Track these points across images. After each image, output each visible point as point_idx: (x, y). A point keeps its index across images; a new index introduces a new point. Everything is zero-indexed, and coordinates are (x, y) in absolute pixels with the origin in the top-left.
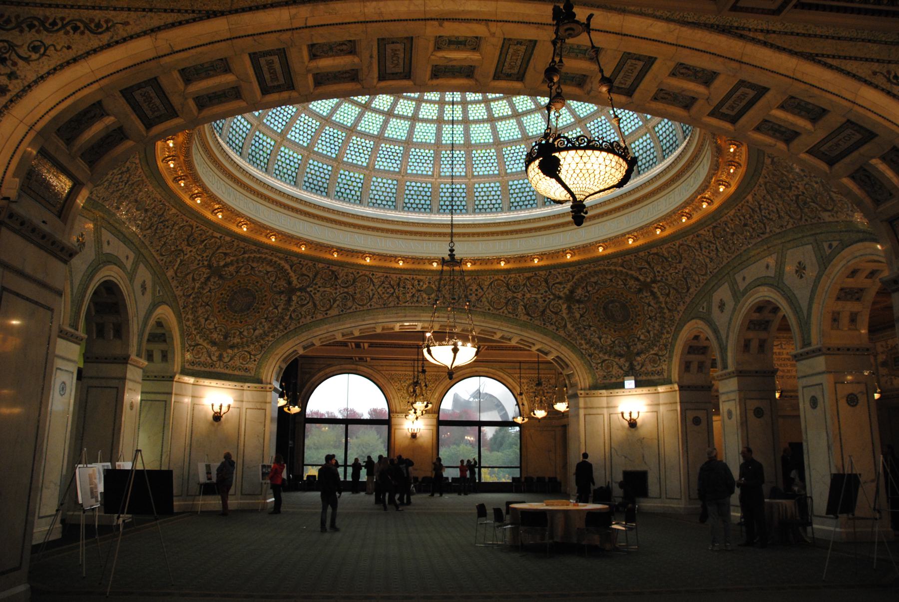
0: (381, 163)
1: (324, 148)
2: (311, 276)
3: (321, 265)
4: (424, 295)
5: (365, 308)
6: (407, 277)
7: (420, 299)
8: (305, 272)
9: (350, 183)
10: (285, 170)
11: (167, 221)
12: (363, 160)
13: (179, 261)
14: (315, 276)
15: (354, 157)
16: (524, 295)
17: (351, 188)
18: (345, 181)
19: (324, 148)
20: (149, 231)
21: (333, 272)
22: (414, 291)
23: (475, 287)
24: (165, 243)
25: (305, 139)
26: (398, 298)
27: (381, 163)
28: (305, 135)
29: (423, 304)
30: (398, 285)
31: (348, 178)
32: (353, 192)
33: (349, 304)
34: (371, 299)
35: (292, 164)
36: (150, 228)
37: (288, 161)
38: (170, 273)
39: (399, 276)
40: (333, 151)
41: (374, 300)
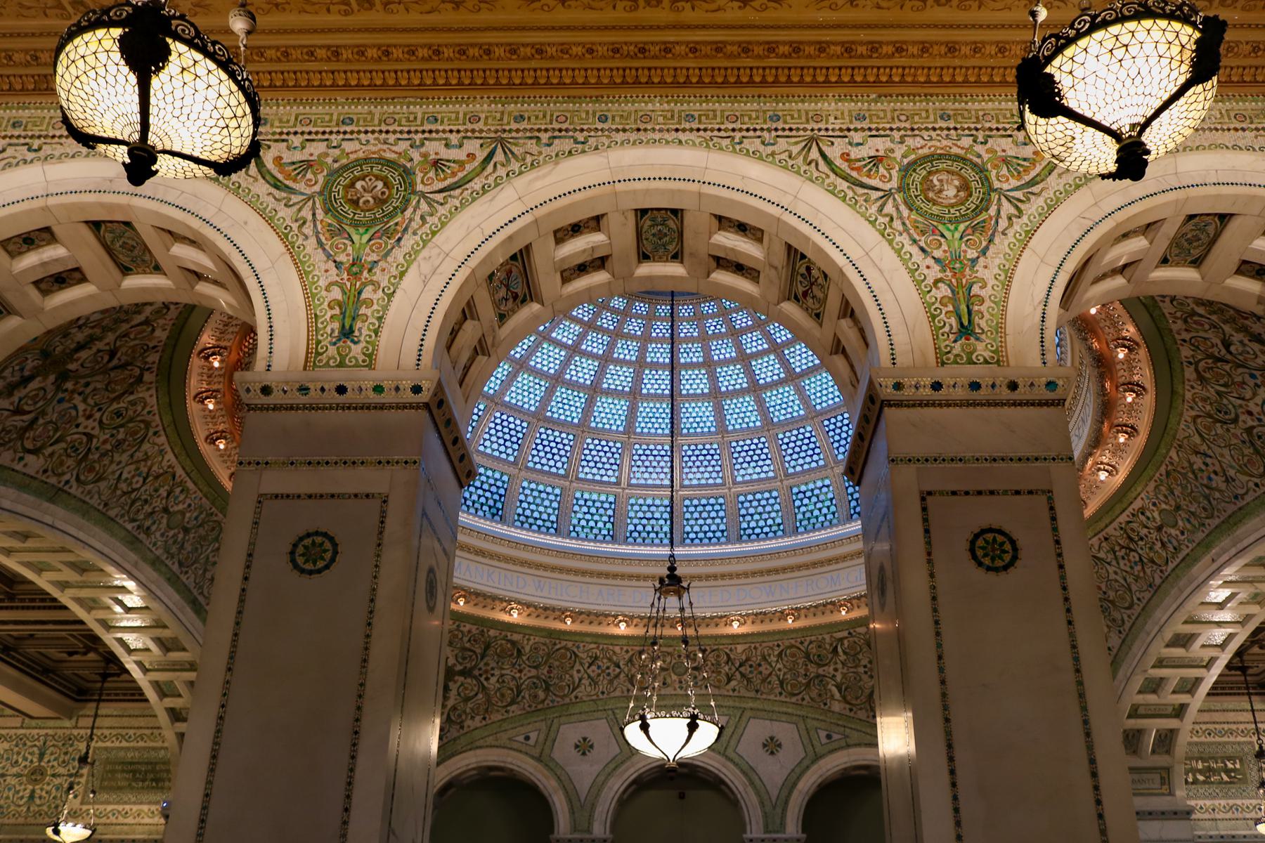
4: (1173, 532)
5: (1137, 609)
6: (1123, 518)
7: (1175, 543)
11: (747, 660)
13: (834, 690)
16: (1250, 413)
20: (733, 683)
22: (1154, 535)
23: (1198, 462)
24: (781, 683)
26: (1153, 562)
29: (1185, 551)
30: (1131, 539)
33: (1117, 615)
34: (1130, 590)
36: (729, 680)
38: (837, 707)
39: (1115, 524)
41: (1134, 588)
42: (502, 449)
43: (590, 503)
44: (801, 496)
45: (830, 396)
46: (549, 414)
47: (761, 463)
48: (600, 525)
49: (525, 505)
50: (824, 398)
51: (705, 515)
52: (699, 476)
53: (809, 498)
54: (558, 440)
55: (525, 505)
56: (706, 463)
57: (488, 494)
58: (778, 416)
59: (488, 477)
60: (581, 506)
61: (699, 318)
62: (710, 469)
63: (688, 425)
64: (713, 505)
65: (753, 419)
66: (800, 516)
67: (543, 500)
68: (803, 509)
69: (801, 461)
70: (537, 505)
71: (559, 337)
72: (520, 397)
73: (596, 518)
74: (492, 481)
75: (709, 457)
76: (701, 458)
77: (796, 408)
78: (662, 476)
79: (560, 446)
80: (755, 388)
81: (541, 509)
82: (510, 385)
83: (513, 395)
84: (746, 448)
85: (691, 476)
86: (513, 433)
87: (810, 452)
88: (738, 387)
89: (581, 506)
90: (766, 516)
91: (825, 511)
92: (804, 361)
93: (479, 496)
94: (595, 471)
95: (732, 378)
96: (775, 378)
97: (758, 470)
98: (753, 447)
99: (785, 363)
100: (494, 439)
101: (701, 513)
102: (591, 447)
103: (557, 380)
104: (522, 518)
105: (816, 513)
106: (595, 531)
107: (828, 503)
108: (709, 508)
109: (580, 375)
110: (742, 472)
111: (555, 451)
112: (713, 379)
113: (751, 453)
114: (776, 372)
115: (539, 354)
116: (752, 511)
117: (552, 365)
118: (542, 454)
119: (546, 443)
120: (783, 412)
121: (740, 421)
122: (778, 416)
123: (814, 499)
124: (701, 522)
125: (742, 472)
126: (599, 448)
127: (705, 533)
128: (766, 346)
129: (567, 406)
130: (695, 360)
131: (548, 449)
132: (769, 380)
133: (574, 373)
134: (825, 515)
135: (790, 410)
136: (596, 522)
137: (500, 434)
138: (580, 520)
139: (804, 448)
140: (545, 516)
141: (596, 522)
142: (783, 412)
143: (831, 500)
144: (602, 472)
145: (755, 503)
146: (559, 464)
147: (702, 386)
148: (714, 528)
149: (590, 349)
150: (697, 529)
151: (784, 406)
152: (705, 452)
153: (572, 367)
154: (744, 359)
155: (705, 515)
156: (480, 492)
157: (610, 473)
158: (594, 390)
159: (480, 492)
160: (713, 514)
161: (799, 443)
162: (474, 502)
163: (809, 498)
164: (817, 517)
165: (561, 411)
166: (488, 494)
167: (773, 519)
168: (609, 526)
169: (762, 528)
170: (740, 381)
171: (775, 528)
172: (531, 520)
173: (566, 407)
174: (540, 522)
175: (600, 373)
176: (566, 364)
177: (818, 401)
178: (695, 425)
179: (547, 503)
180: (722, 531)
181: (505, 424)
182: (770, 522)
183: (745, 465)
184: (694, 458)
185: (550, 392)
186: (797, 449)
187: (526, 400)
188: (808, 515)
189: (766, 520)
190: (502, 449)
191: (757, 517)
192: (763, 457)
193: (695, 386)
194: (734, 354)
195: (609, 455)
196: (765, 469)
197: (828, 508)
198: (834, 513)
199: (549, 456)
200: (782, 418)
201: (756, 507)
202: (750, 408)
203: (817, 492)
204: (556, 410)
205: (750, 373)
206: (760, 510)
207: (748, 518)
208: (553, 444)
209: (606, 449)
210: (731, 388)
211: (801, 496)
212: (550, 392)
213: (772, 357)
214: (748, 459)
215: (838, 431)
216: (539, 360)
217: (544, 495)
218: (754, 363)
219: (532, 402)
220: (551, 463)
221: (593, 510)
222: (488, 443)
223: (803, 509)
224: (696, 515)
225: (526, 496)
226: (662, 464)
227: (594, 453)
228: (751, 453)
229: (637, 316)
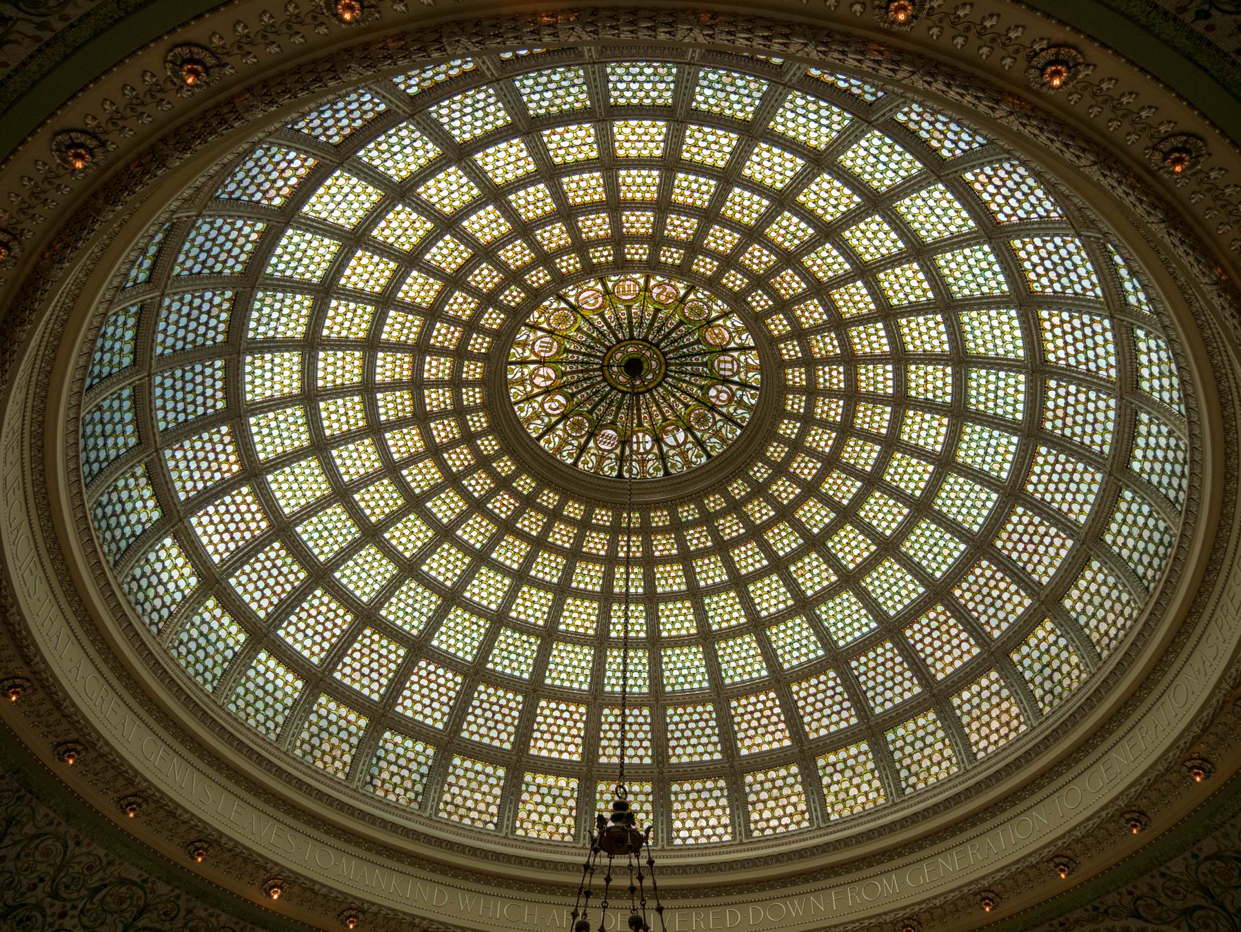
0: (1041, 569)
1: (948, 659)
2: (1203, 902)
3: (1176, 867)
8: (1179, 905)
9: (1046, 659)
10: (926, 763)
12: (1016, 599)
14: (1206, 891)
15: (1001, 615)
17: (1056, 664)
18: (1037, 666)
19: (948, 659)
21: (1216, 856)
25: (907, 684)
27: (1041, 569)
28: (899, 679)
31: (1035, 654)
32: (1065, 668)
35: (929, 739)
37: (919, 745)
40: (965, 646)
42: (428, 711)
43: (544, 790)
44: (830, 770)
45: (856, 625)
46: (490, 666)
47: (771, 728)
48: (558, 820)
49: (455, 790)
50: (848, 629)
51: (700, 804)
52: (690, 750)
53: (842, 772)
54: (503, 702)
55: (455, 790)
56: (698, 732)
57: (405, 773)
58: (790, 661)
59: (406, 749)
60: (532, 794)
61: (677, 528)
62: (704, 740)
63: (672, 680)
64: (710, 790)
65: (757, 667)
66: (830, 799)
67: (480, 784)
68: (834, 788)
69: (825, 722)
70: (473, 791)
71: (501, 559)
72: (452, 641)
73: (552, 810)
74: (411, 755)
75: (702, 724)
76: (692, 725)
77: (812, 647)
78: (641, 752)
79: (506, 711)
80: (757, 625)
81: (478, 796)
82: (440, 624)
83: (444, 638)
84: (750, 708)
85: (679, 751)
86: (442, 690)
87: (836, 708)
88: (733, 623)
89: (532, 794)
90: (783, 801)
91: (865, 787)
92: (817, 580)
93: (393, 774)
94: (551, 745)
95: (725, 611)
96: (781, 606)
97: (769, 738)
98: (760, 706)
99: (792, 585)
100: (417, 697)
101: (694, 801)
102: (547, 712)
103: (499, 619)
104: (449, 808)
105: (853, 791)
106: (549, 828)
107: (868, 777)
108: (705, 795)
109: (530, 612)
110: (747, 742)
111: (498, 717)
112: (701, 615)
113: (757, 715)
114: (782, 598)
115: (475, 582)
116: (764, 795)
117: (493, 598)
118: (481, 721)
119: (486, 706)
120: (795, 654)
121: (739, 670)
122: (790, 661)
123: (848, 773)
124: (695, 814)
125: (747, 742)
126: (557, 713)
127: (702, 829)
128: (765, 562)
129: (514, 656)
130: (675, 588)
131: (489, 714)
132: (773, 610)
133: (521, 609)
134: (866, 794)
135: (804, 650)
136: (552, 816)
137: (425, 691)
138: (530, 812)
139: (828, 702)
140: (482, 807)
141: (552, 816)
142: (795, 654)
143: (872, 771)
144: (562, 747)
145: (768, 785)
146: (504, 736)
147: (687, 624)
148: (713, 822)
149: (540, 575)
150: (689, 824)
151: (796, 645)
152: (696, 717)
153: (519, 601)
154: (738, 583)
155: (700, 804)
156: (394, 768)
157: (572, 748)
158: (549, 635)
159: (394, 768)
160: (712, 803)
161: (820, 696)
162: (384, 781)
163: (842, 772)
164: (855, 797)
165: (506, 662)
166: (405, 773)
167: (794, 805)
168: (570, 821)
169: (779, 819)
170: (735, 615)
171: (797, 818)
172: (462, 811)
173: (513, 657)
174: (474, 815)
175: (556, 611)
176: (511, 596)
177: (841, 634)
178: (681, 679)
179: (485, 788)
180: (725, 826)
181: (433, 677)
182: (790, 809)
183: (751, 733)
184: (682, 726)
185: (490, 639)
186: (819, 705)
187: (460, 645)
188: (842, 796)
189: (784, 807)
190: (428, 711)
191: (771, 804)
192: (774, 719)
193: (678, 625)
194: (725, 577)
195: (570, 723)
196: (778, 735)
197: (869, 783)
198: (877, 790)
199: (491, 724)
200: (795, 662)
201: (769, 791)
202: (752, 652)
203: (851, 762)
204: (498, 662)
205: (748, 604)
206: (775, 792)
207: (760, 806)
208: (496, 708)
209: (566, 715)
210: (724, 625)
211: (830, 770)
212: (490, 639)
213: (775, 578)
214: (754, 723)
215: (871, 674)
216: (476, 590)
217: (482, 778)
218: (751, 588)
219: (468, 649)
220: (494, 733)
221: (549, 800)
222: (408, 703)
223: (834, 788)
224: (688, 805)
225: (458, 777)
226: (641, 735)
227: (550, 720)
228: (757, 715)
229: (599, 529)
